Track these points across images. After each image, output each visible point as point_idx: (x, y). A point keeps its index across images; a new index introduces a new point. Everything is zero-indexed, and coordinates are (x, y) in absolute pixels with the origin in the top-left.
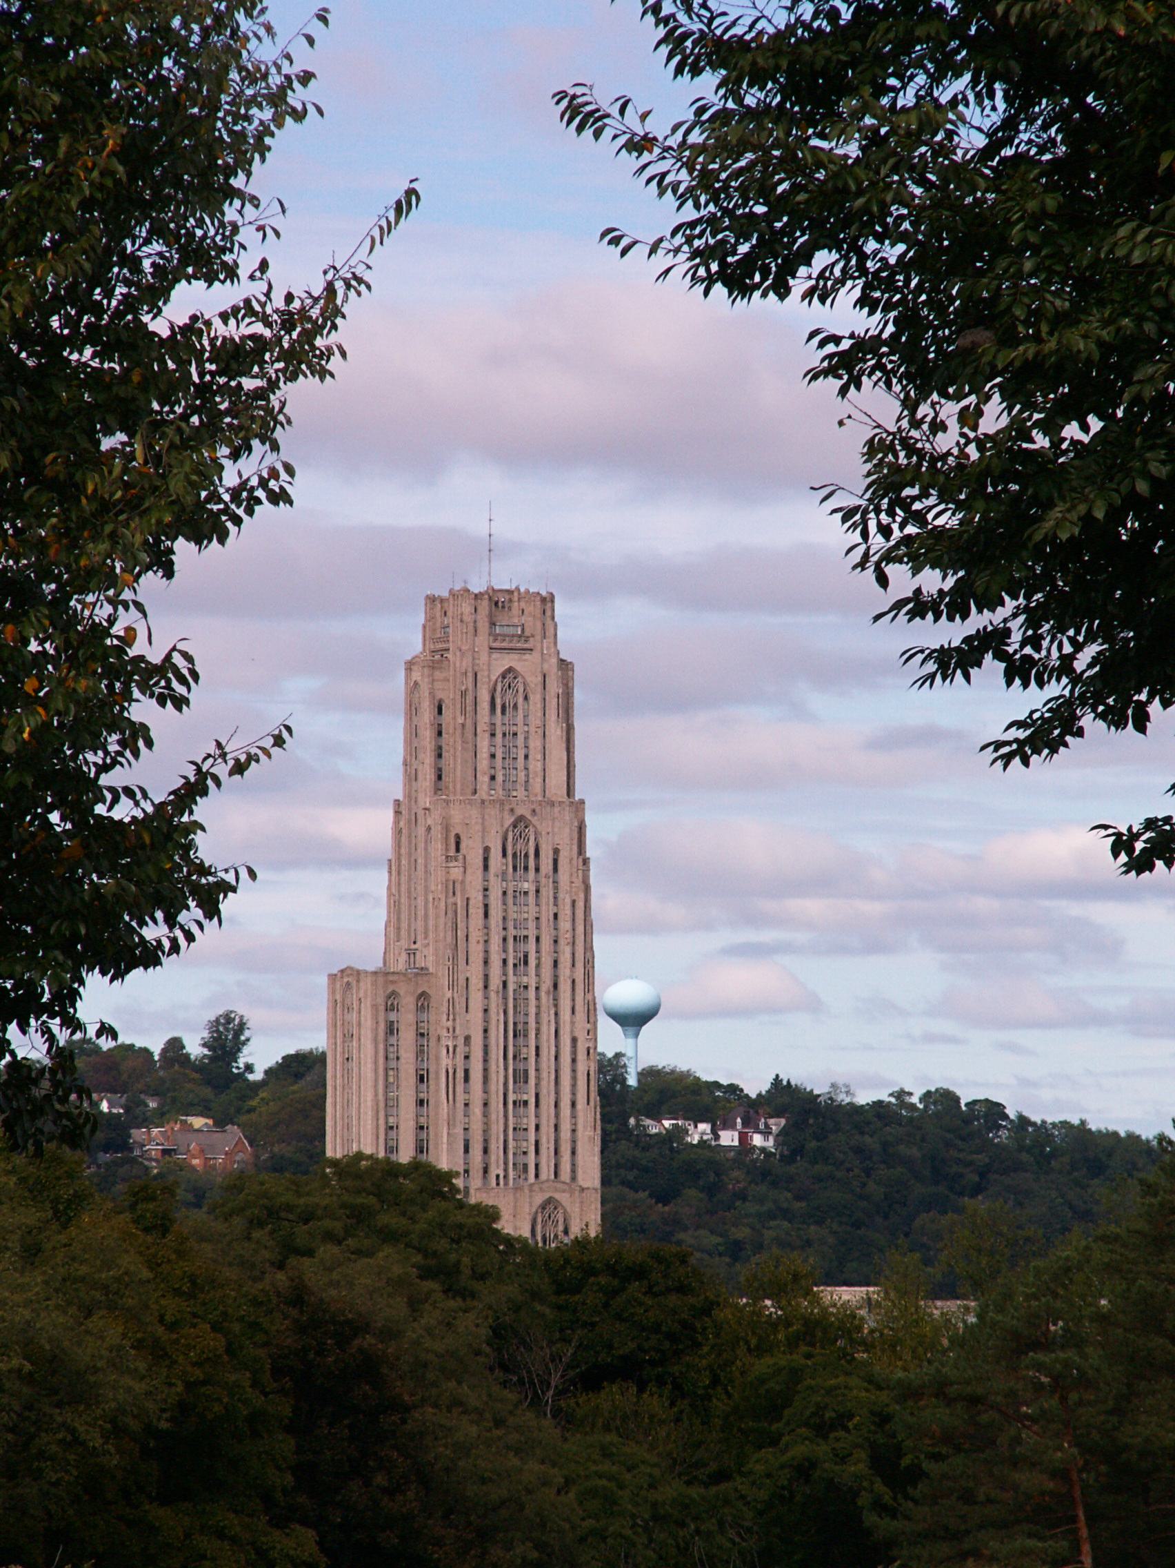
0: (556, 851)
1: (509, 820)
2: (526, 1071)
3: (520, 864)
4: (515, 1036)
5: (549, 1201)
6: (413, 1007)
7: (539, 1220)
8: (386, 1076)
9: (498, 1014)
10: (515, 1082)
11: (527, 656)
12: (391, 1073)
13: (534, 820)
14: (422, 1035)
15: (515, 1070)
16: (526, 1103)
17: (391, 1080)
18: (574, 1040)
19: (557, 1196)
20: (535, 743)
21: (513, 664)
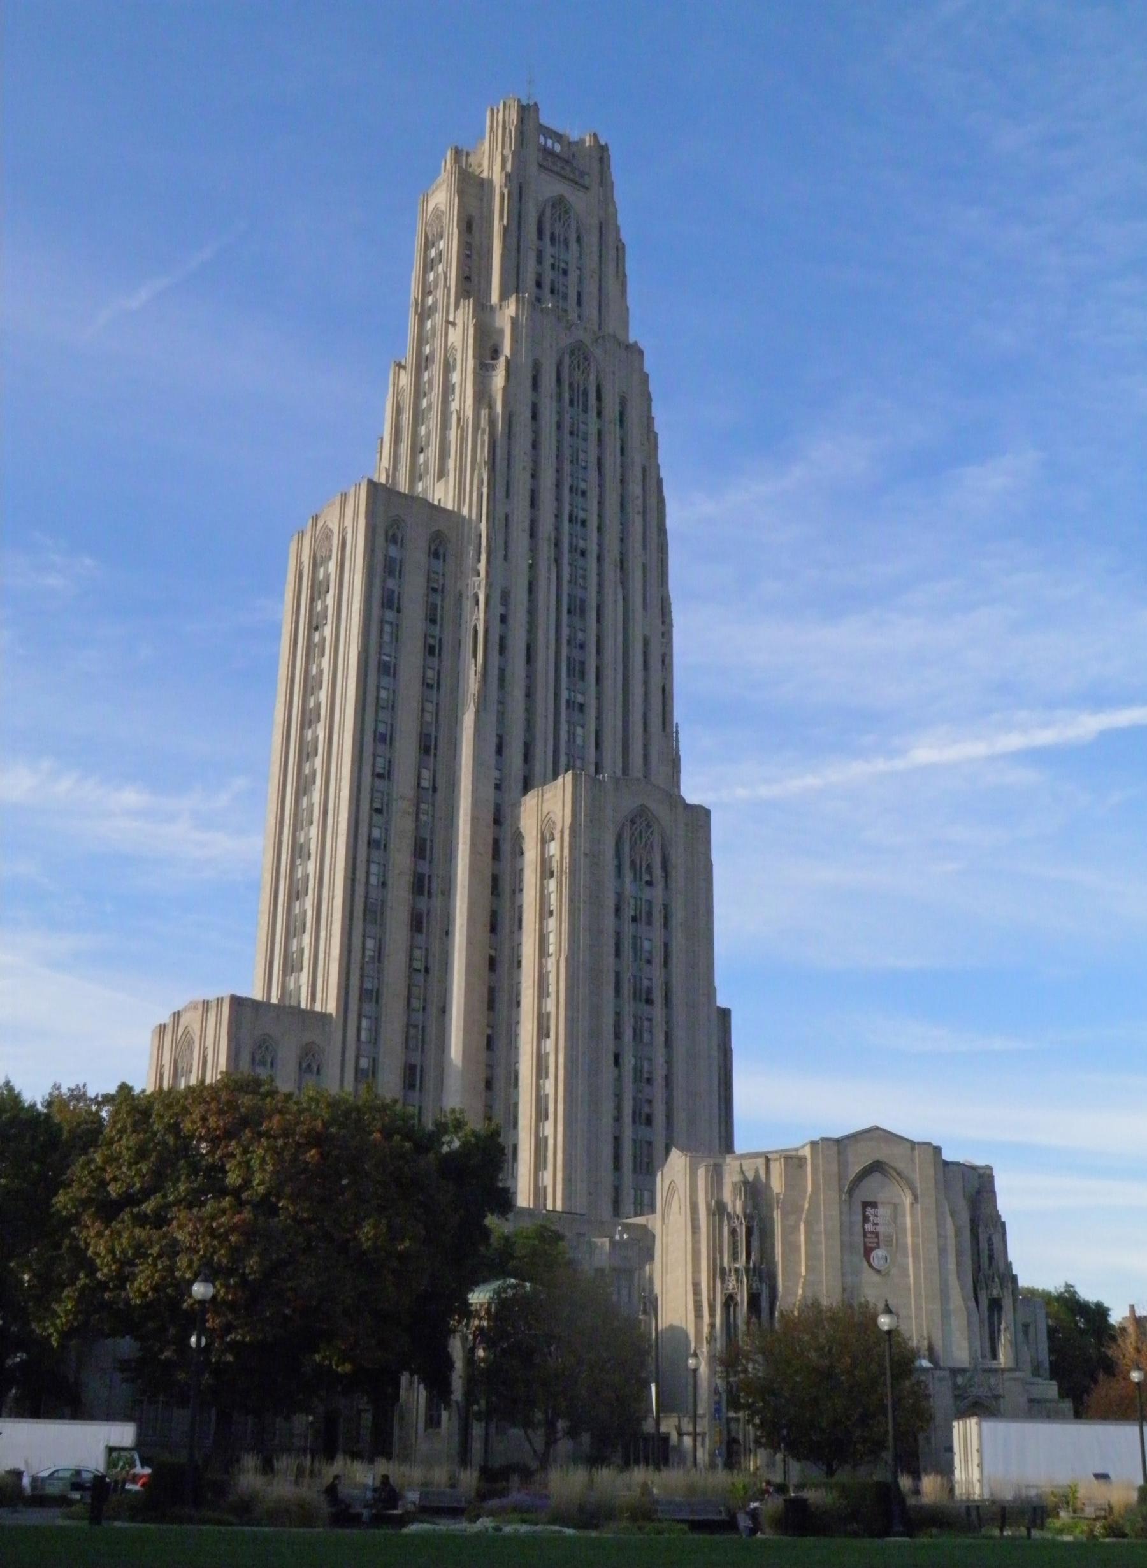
0: (623, 402)
1: (566, 341)
2: (582, 663)
3: (578, 399)
4: (569, 612)
5: (642, 811)
6: (423, 544)
7: (627, 835)
8: (381, 631)
9: (549, 570)
10: (569, 675)
11: (581, 194)
12: (387, 628)
13: (598, 352)
14: (434, 590)
15: (569, 658)
16: (581, 707)
17: (386, 638)
18: (646, 643)
19: (652, 806)
20: (591, 288)
21: (567, 195)
